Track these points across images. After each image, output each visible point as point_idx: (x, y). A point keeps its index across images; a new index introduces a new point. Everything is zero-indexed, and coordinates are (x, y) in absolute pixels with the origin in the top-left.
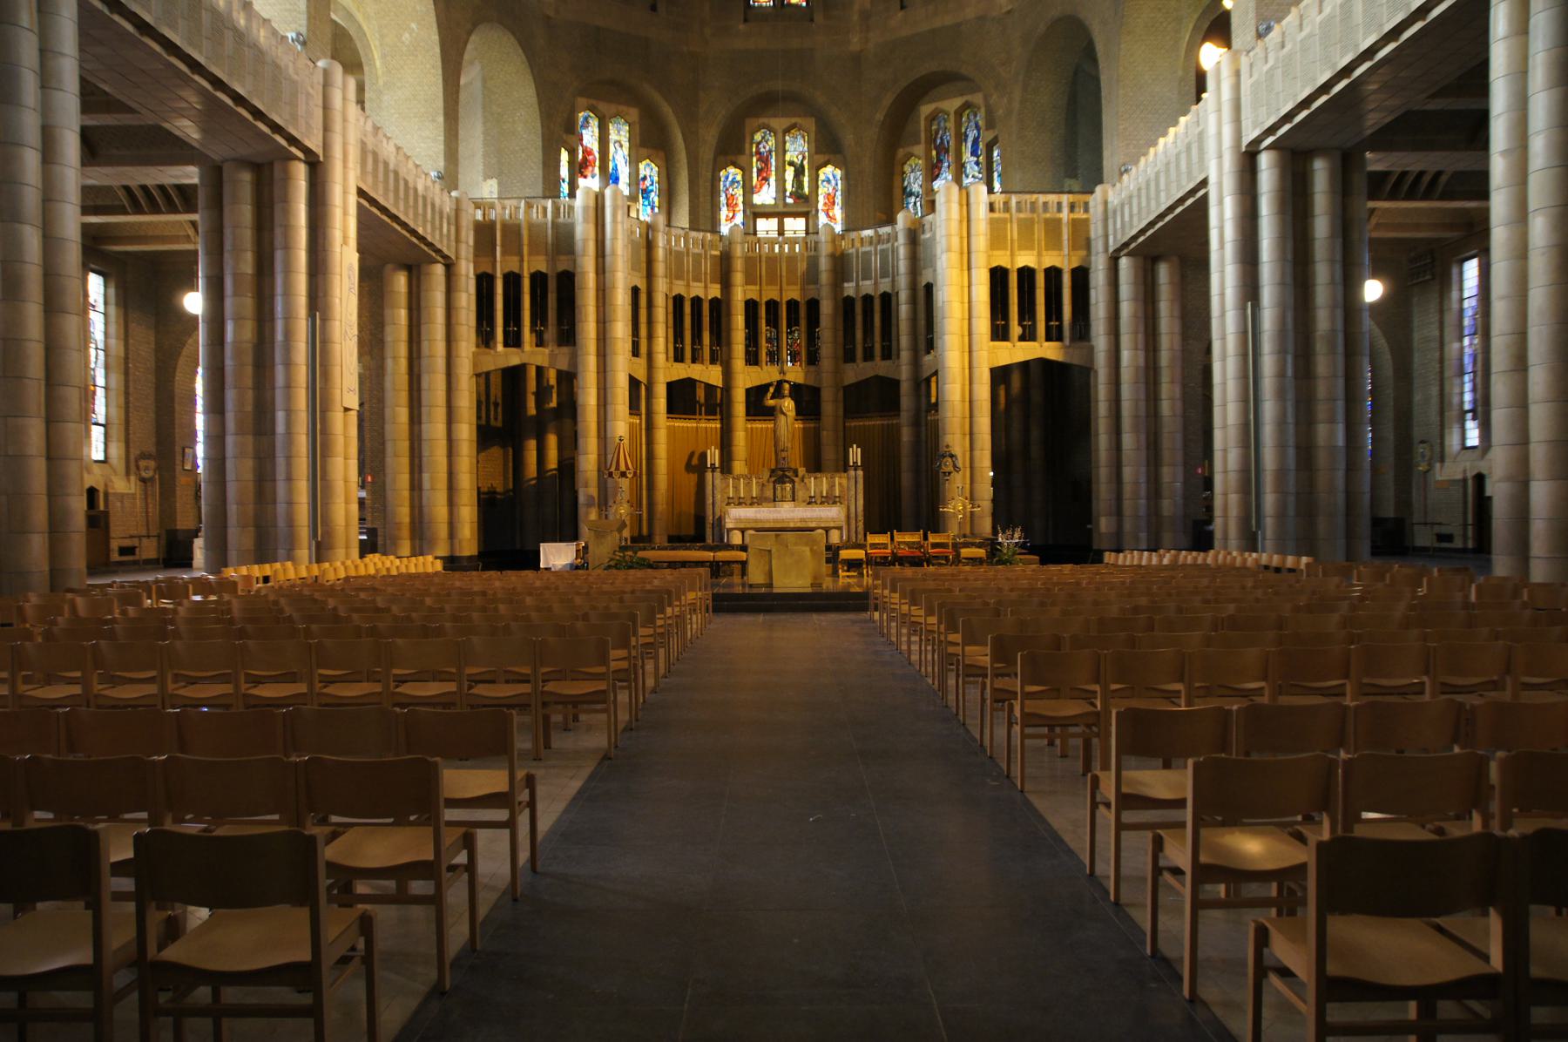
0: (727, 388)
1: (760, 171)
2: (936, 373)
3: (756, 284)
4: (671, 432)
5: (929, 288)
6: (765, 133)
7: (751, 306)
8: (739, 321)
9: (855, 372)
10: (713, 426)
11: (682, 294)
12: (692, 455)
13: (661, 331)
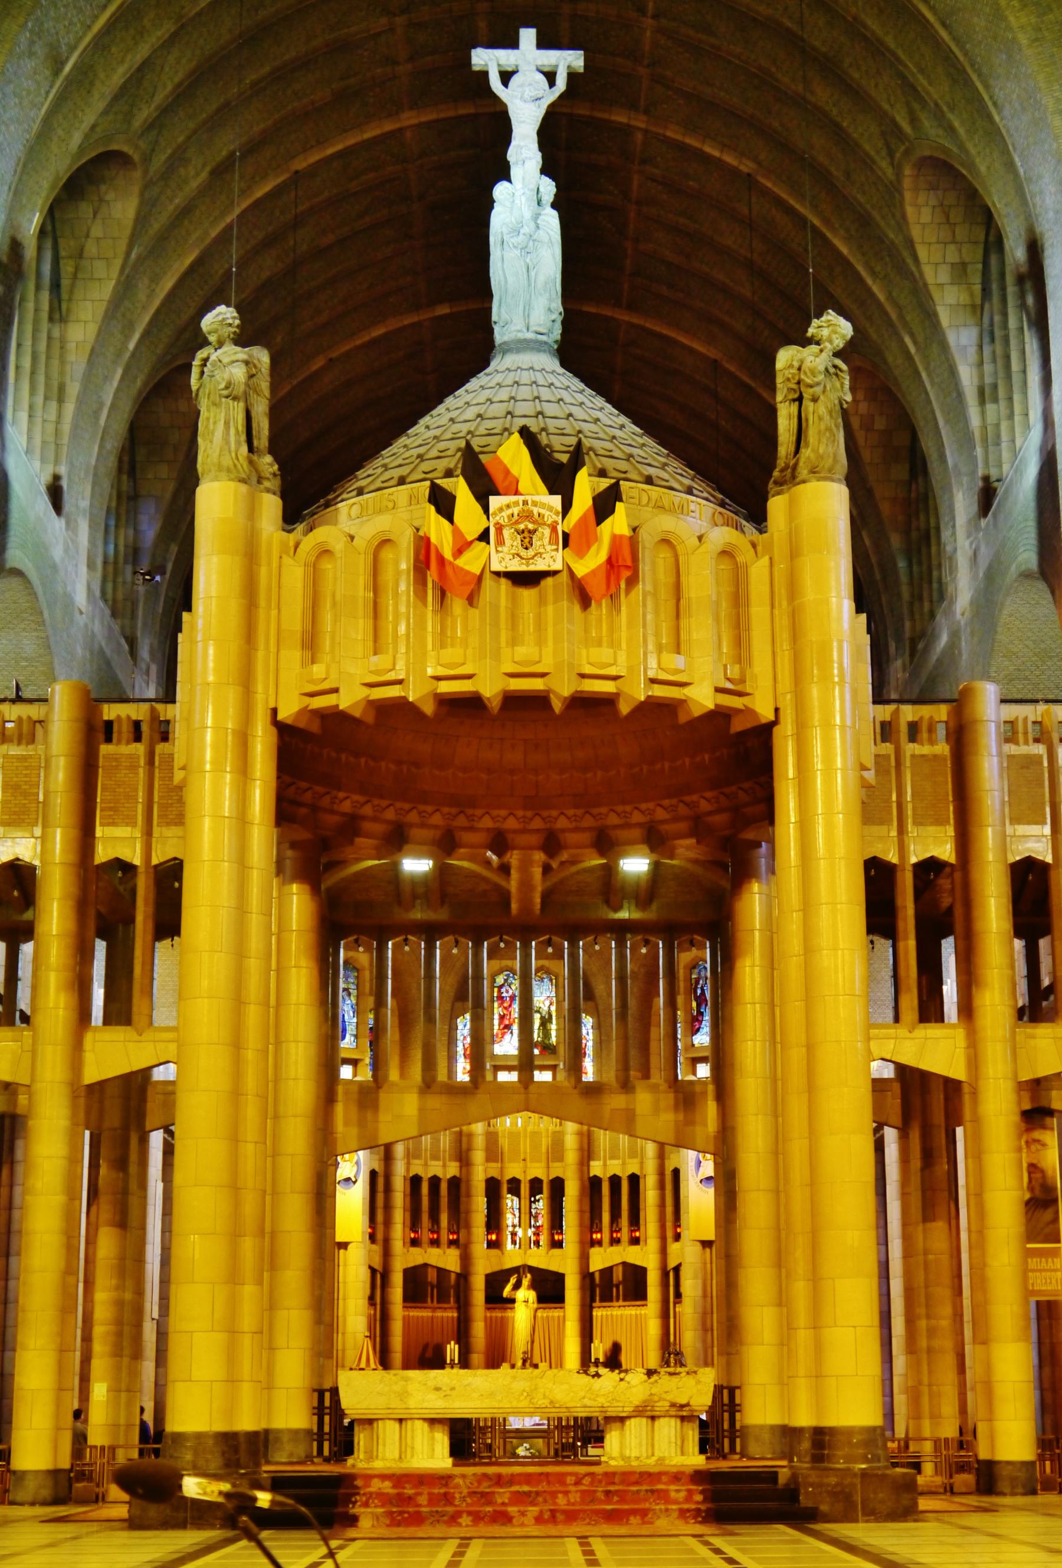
0: (464, 1276)
1: (502, 1018)
2: (680, 1265)
3: (497, 1161)
4: (406, 1320)
5: (676, 1172)
6: (508, 975)
7: (493, 1188)
8: (480, 1204)
9: (600, 1259)
10: (450, 1315)
11: (420, 1174)
12: (426, 1347)
13: (399, 1216)
